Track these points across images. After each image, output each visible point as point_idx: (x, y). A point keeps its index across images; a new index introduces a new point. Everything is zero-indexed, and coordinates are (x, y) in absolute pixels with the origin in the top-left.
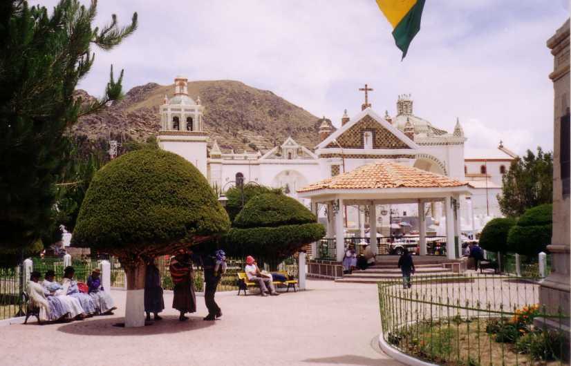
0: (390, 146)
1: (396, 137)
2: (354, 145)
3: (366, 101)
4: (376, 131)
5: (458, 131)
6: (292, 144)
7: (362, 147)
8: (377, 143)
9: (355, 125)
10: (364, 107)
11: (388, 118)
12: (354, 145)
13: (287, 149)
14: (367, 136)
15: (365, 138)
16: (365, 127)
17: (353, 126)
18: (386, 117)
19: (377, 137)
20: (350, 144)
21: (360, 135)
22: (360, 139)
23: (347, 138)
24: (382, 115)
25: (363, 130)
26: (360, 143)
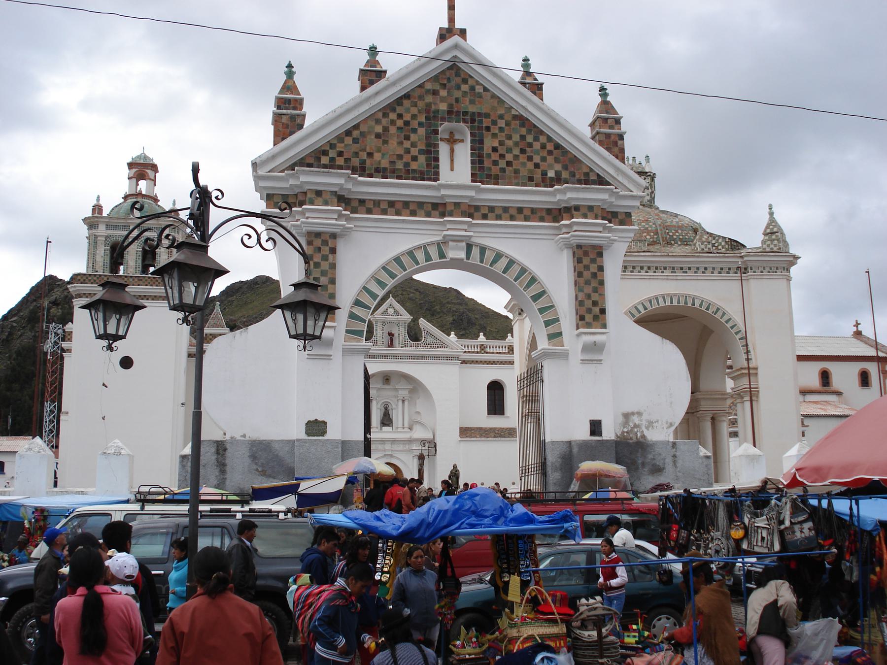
0: (538, 176)
1: (558, 146)
2: (400, 165)
3: (451, 20)
4: (486, 122)
5: (773, 232)
6: (397, 313)
7: (431, 173)
8: (487, 163)
9: (407, 96)
10: (444, 35)
11: (529, 80)
12: (400, 165)
13: (384, 323)
14: (452, 141)
15: (443, 150)
16: (443, 107)
17: (399, 101)
18: (523, 78)
19: (489, 143)
20: (385, 164)
21: (422, 131)
22: (422, 146)
23: (371, 142)
24: (517, 76)
25: (432, 117)
26: (422, 159)
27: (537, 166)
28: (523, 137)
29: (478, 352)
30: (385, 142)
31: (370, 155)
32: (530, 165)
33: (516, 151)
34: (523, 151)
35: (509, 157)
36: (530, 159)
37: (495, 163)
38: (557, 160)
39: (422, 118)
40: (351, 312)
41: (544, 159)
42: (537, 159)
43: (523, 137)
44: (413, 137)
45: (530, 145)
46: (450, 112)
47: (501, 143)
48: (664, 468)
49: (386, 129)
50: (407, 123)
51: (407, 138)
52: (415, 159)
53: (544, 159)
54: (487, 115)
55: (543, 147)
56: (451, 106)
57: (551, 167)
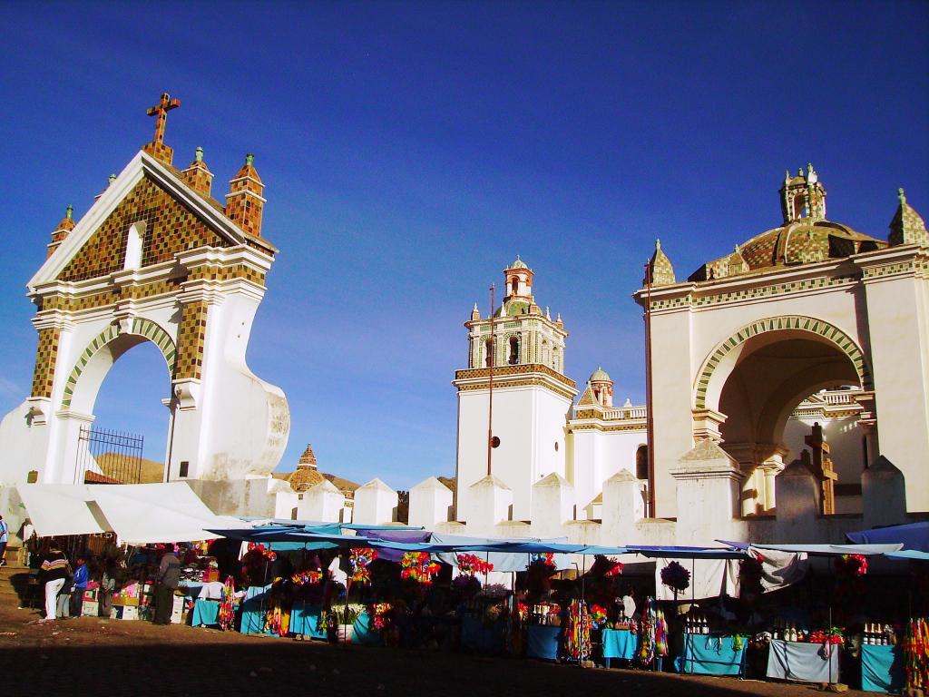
16: (135, 211)
27: (183, 241)
28: (178, 219)
29: (849, 403)
30: (100, 250)
31: (90, 263)
32: (179, 241)
33: (172, 233)
34: (176, 231)
35: (167, 239)
36: (179, 236)
37: (157, 247)
38: (196, 233)
39: (121, 225)
40: (67, 388)
41: (188, 234)
42: (183, 236)
43: (178, 219)
44: (115, 240)
45: (181, 224)
46: (138, 214)
47: (164, 229)
48: (238, 506)
49: (101, 240)
50: (113, 231)
51: (111, 243)
52: (113, 258)
53: (188, 234)
54: (158, 209)
55: (189, 223)
56: (139, 209)
57: (191, 239)
